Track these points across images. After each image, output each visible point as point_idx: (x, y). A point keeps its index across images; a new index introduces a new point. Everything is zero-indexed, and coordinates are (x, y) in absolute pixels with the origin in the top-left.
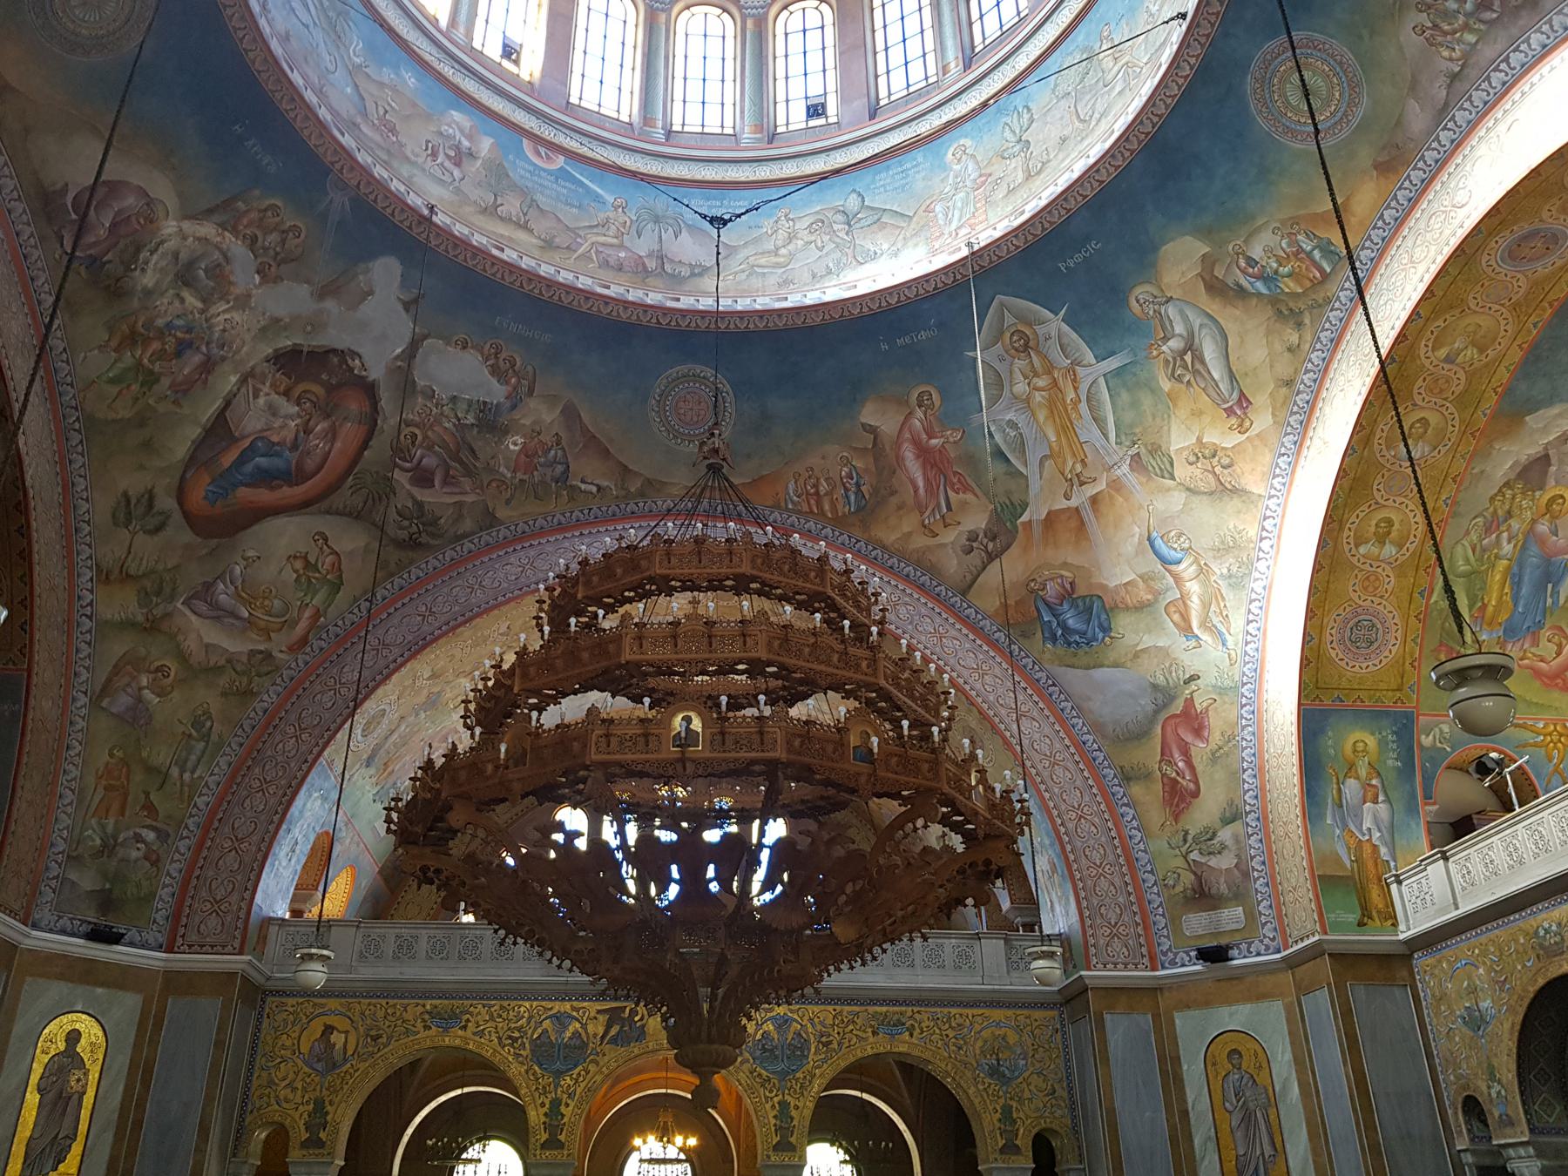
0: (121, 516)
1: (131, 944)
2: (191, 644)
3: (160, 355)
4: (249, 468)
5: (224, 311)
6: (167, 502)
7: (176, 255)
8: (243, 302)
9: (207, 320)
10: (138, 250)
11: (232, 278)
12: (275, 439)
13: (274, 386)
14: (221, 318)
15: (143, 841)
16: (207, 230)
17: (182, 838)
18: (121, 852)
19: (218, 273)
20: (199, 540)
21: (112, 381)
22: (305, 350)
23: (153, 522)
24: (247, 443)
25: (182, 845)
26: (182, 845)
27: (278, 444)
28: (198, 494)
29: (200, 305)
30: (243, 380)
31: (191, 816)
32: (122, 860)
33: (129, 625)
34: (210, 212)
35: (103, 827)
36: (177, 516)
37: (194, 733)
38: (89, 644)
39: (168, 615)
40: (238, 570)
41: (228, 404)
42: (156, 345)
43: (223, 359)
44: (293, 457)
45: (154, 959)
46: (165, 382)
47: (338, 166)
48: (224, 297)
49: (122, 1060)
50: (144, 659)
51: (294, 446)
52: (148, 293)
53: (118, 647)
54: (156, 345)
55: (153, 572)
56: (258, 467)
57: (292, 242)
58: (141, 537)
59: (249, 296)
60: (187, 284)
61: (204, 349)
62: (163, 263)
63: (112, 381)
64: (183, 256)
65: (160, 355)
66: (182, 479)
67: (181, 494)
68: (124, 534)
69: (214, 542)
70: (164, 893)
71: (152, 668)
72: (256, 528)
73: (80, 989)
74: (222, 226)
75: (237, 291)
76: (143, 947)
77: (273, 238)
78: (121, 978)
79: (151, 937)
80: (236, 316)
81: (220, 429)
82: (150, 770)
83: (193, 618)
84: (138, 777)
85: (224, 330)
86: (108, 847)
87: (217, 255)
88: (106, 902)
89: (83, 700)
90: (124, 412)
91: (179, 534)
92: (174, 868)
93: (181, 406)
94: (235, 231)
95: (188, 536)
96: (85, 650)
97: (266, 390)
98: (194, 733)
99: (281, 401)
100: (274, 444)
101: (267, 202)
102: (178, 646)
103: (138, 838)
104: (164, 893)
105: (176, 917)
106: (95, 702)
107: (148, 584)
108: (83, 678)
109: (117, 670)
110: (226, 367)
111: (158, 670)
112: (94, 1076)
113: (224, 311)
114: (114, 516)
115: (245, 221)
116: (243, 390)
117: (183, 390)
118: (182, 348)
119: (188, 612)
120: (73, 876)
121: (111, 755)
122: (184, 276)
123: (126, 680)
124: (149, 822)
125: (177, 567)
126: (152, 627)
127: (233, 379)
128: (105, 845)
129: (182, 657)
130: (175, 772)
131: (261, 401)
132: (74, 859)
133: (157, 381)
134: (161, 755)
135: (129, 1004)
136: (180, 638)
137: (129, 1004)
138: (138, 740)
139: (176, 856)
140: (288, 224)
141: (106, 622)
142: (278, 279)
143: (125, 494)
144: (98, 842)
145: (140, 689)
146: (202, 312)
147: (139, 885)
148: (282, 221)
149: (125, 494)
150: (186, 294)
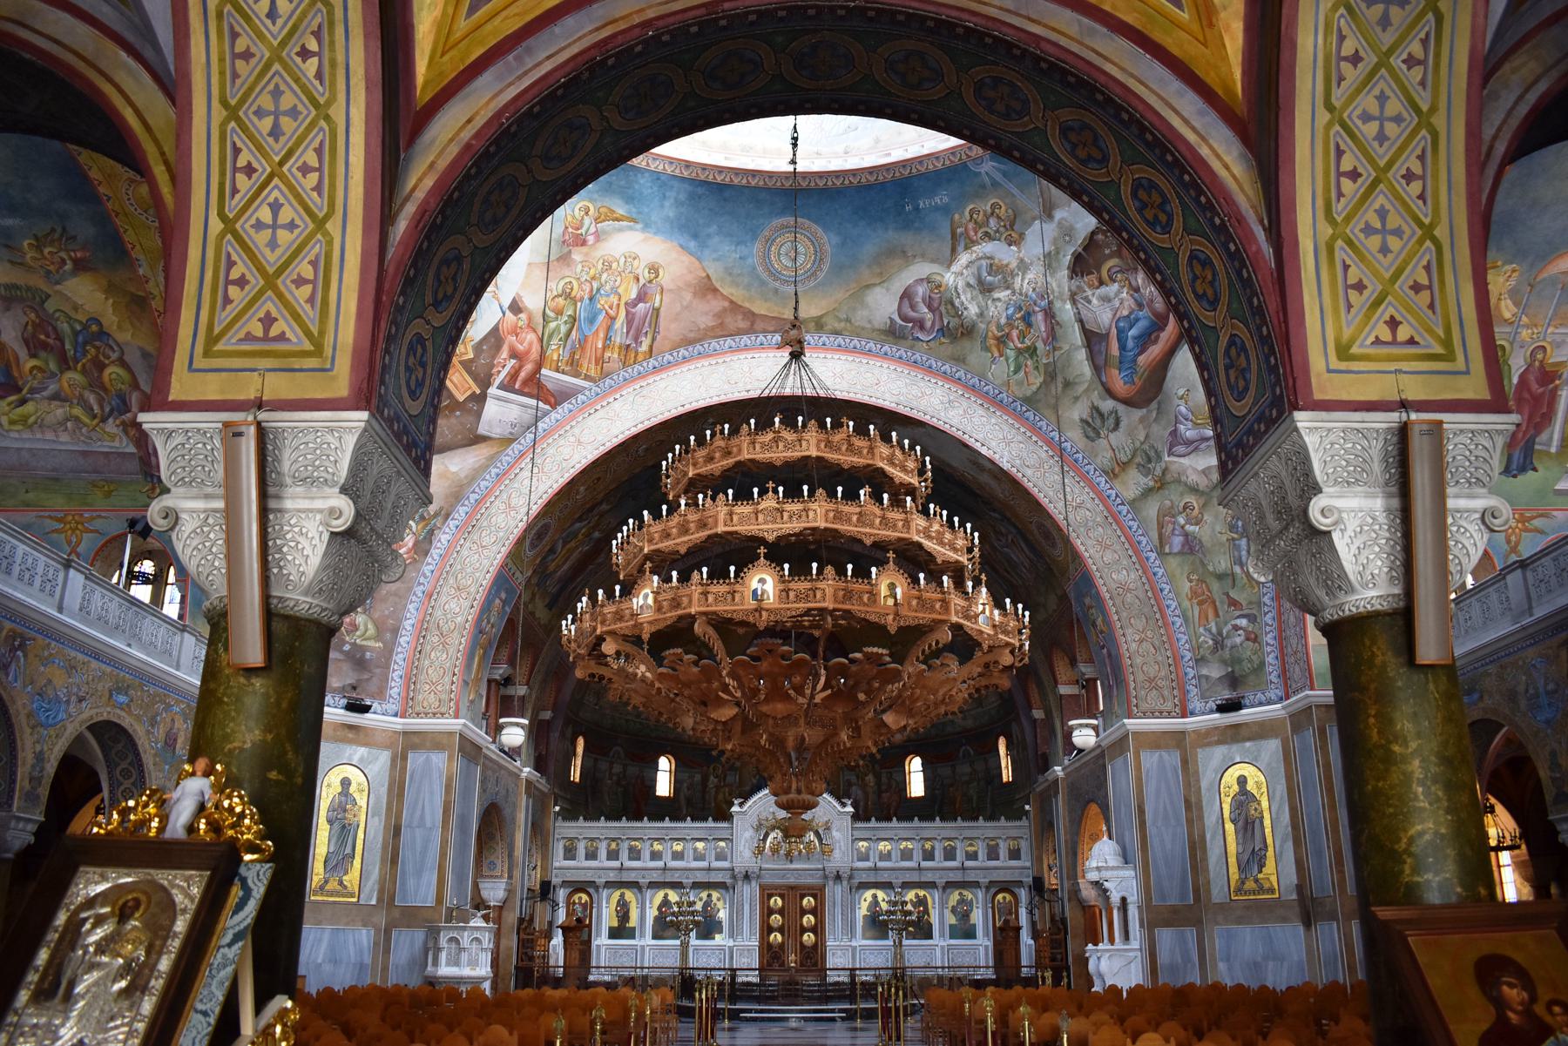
0: (1092, 434)
1: (1252, 706)
2: (1193, 478)
3: (1022, 336)
4: (1130, 344)
5: (1023, 280)
6: (1108, 405)
7: (969, 285)
8: (1023, 266)
9: (1021, 294)
10: (952, 304)
11: (1005, 262)
12: (1125, 313)
13: (1091, 286)
14: (1025, 285)
15: (1241, 628)
16: (964, 258)
17: (1266, 614)
18: (1228, 643)
19: (994, 268)
20: (1145, 410)
21: (1016, 372)
22: (1080, 250)
23: (1111, 421)
24: (1114, 331)
25: (1268, 619)
26: (1268, 619)
27: (1131, 313)
28: (1118, 381)
29: (1009, 292)
30: (1074, 302)
31: (1264, 595)
32: (1232, 647)
33: (1148, 492)
34: (954, 251)
35: (1210, 631)
36: (1121, 408)
37: (1235, 536)
38: (1133, 520)
39: (1165, 471)
40: (1183, 409)
41: (1081, 321)
42: (1015, 333)
43: (1050, 303)
44: (1145, 312)
45: (1275, 710)
46: (1040, 345)
47: (964, 157)
48: (1013, 275)
49: (1281, 788)
50: (1172, 507)
51: (1140, 306)
52: (981, 315)
53: (1152, 509)
54: (1015, 333)
55: (1135, 451)
56: (1135, 338)
57: (1002, 212)
58: (1112, 436)
59: (1022, 260)
60: (990, 290)
61: (1037, 309)
62: (969, 296)
63: (1016, 372)
64: (972, 281)
65: (1022, 336)
66: (1103, 384)
67: (1110, 393)
68: (1103, 442)
69: (1154, 405)
70: (1270, 659)
71: (1181, 509)
72: (1170, 374)
73: (1235, 747)
74: (967, 248)
75: (1014, 264)
76: (1269, 703)
77: (993, 222)
78: (1261, 731)
79: (1273, 694)
80: (1030, 276)
81: (1093, 339)
82: (1220, 577)
83: (1182, 460)
84: (1215, 586)
85: (1034, 289)
86: (1219, 644)
87: (984, 262)
88: (1233, 681)
89: (1153, 555)
90: (1037, 380)
91: (1130, 417)
92: (1269, 638)
93: (1060, 348)
94: (974, 243)
95: (1138, 414)
96: (1135, 525)
97: (1089, 293)
98: (1235, 536)
99: (1103, 290)
100: (1128, 316)
101: (967, 213)
102: (1186, 484)
103: (1236, 628)
104: (1270, 659)
105: (1284, 674)
106: (1161, 554)
107: (1138, 459)
108: (1144, 542)
109: (1161, 526)
110: (1058, 304)
111: (1185, 508)
112: (1265, 804)
113: (1023, 280)
114: (1087, 437)
115: (972, 233)
116: (1080, 306)
117: (1053, 335)
118: (1027, 319)
119: (1175, 459)
120: (1204, 672)
121: (1191, 581)
122: (985, 289)
123: (1170, 527)
124: (1238, 613)
125: (1147, 436)
126: (1162, 484)
127: (1068, 306)
128: (1216, 643)
129: (1194, 490)
130: (1237, 569)
131: (1095, 301)
132: (1200, 661)
133: (1035, 349)
134: (1222, 563)
135: (1272, 746)
136: (1183, 478)
137: (1272, 746)
138: (1202, 562)
139: (1268, 629)
140: (989, 210)
141: (1134, 500)
142: (1022, 236)
143: (1082, 420)
144: (1211, 642)
145: (1183, 527)
146: (1014, 293)
147: (1250, 661)
148: (985, 211)
149: (1082, 420)
150: (996, 295)
